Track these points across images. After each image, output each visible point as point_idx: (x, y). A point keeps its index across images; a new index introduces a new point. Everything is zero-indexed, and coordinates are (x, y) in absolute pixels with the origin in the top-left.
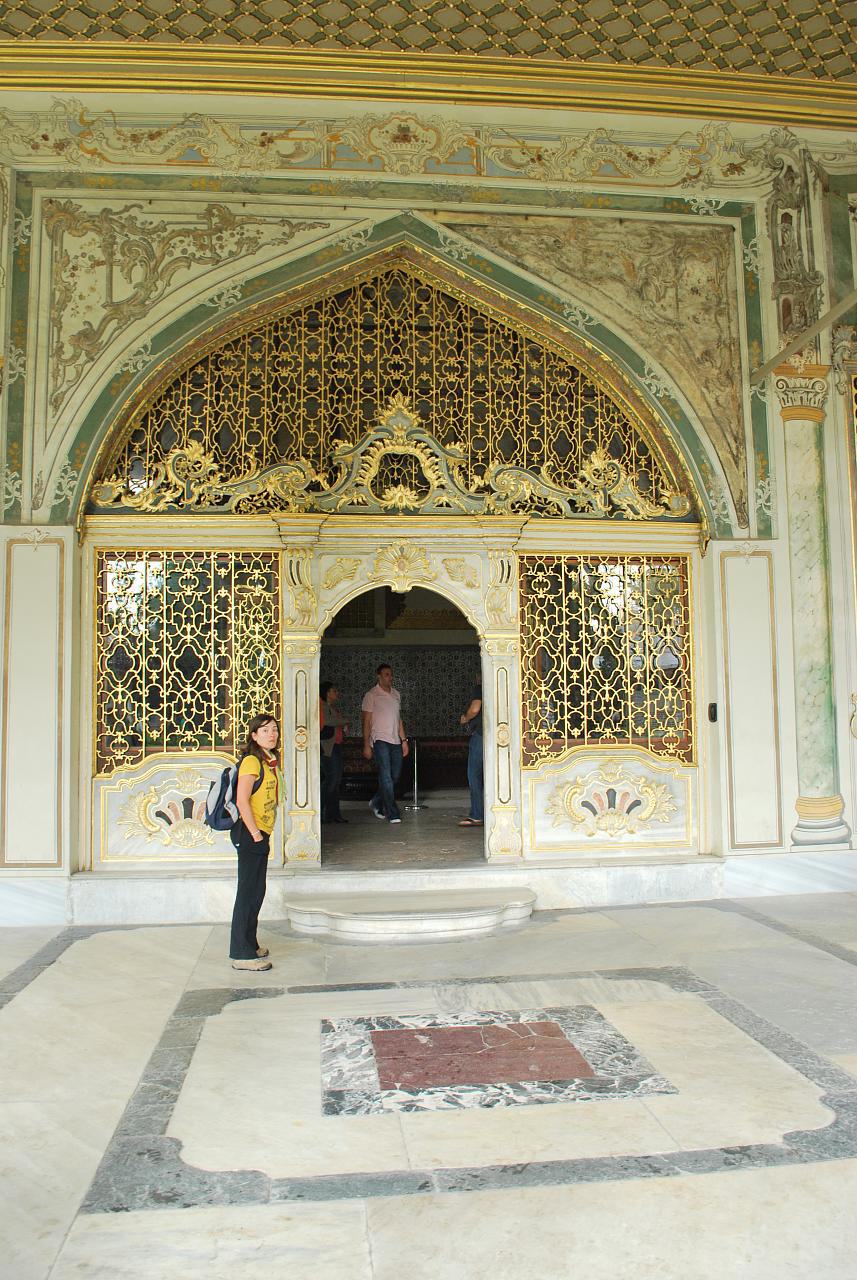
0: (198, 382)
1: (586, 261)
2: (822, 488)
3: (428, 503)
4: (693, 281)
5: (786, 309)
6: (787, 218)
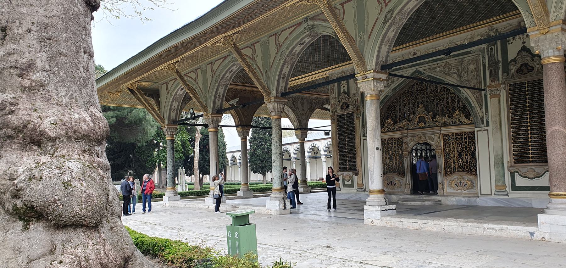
0: (391, 107)
1: (449, 71)
2: (500, 114)
3: (426, 126)
4: (470, 70)
5: (491, 72)
6: (492, 49)
